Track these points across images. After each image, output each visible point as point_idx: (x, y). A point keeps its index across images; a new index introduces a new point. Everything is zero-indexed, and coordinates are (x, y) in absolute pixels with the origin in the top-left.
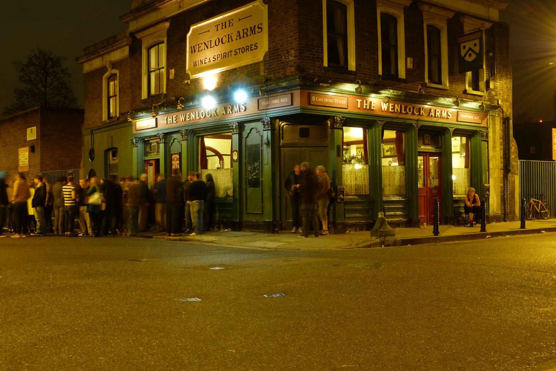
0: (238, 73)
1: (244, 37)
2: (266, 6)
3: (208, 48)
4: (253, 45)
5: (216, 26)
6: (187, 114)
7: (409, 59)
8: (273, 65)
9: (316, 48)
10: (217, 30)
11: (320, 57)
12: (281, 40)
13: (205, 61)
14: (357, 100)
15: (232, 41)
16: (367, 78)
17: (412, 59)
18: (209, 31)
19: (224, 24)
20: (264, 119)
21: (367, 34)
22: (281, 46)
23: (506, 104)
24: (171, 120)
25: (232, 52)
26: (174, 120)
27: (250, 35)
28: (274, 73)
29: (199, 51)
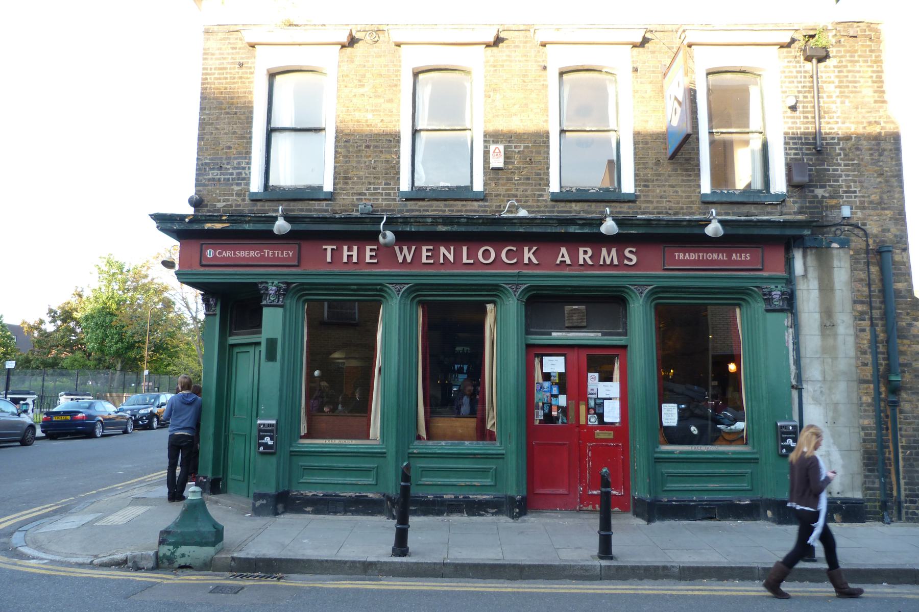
6: (424, 248)
24: (355, 253)
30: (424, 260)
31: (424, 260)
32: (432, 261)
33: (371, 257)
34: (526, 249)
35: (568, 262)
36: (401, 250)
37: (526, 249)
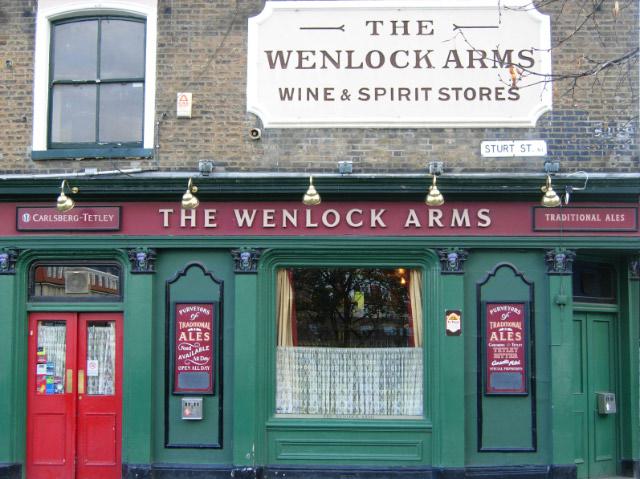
0: (450, 141)
1: (471, 66)
2: (546, 19)
3: (337, 65)
4: (503, 88)
5: (371, 25)
6: (266, 212)
8: (566, 141)
10: (375, 33)
13: (326, 94)
15: (430, 66)
18: (341, 28)
19: (400, 24)
20: (557, 249)
22: (590, 107)
25: (429, 92)
27: (495, 67)
28: (572, 159)
29: (300, 66)
30: (266, 224)
31: (266, 224)
32: (273, 225)
33: (211, 221)
34: (373, 211)
35: (418, 225)
36: (241, 214)
37: (373, 211)
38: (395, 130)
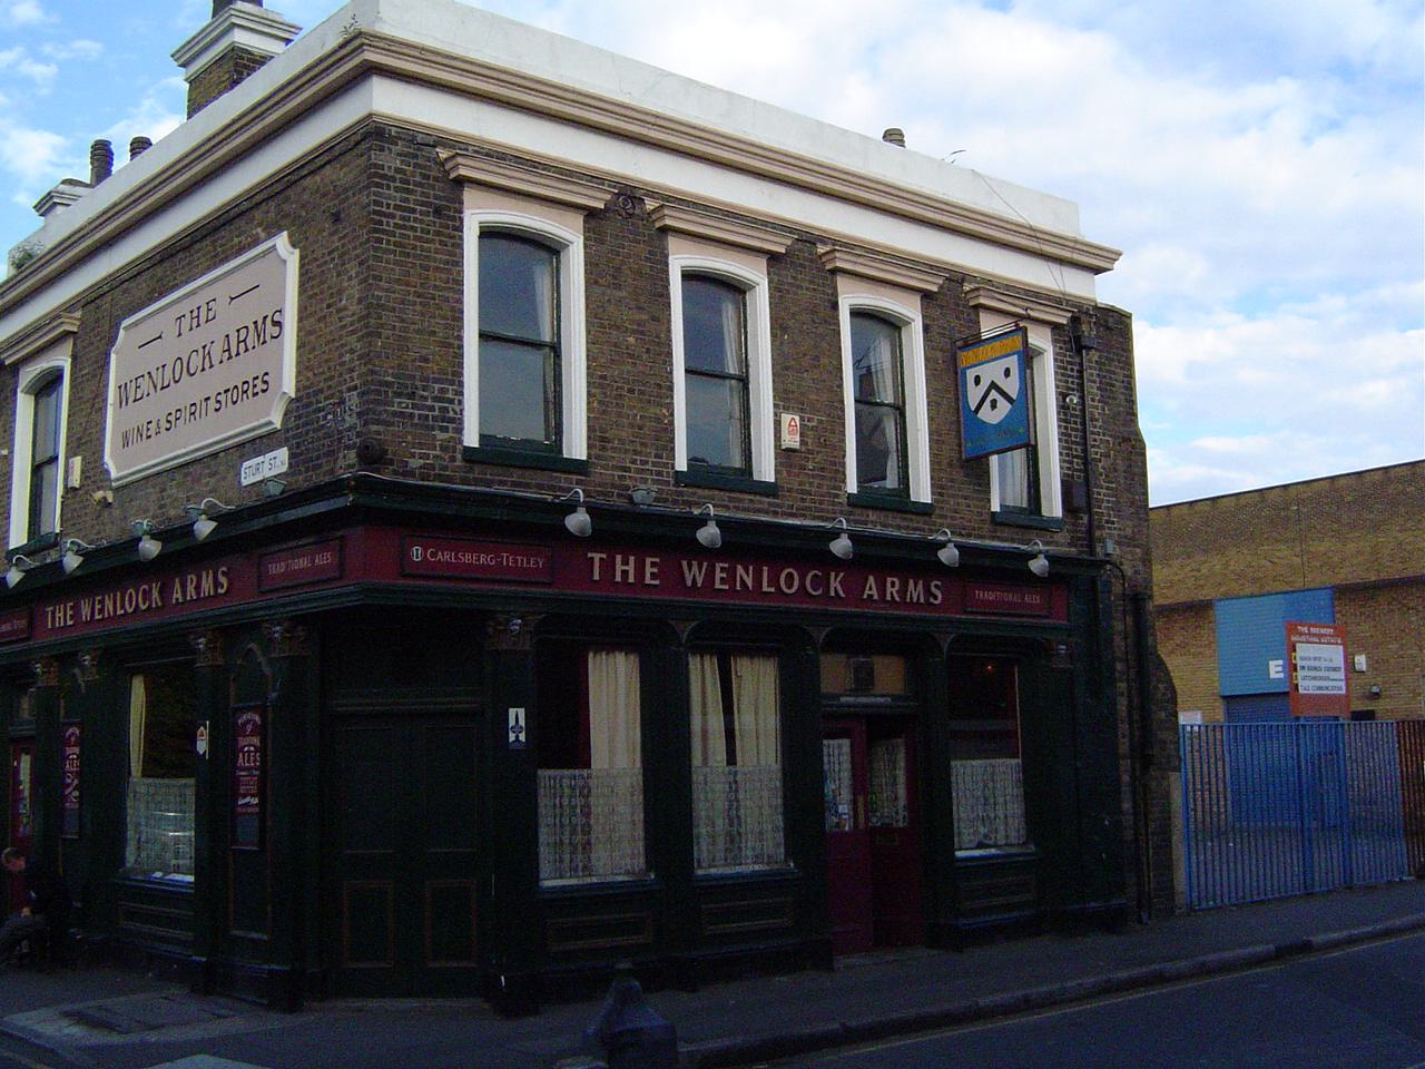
1: (238, 354)
2: (297, 251)
4: (257, 378)
7: (786, 418)
9: (437, 386)
11: (451, 414)
12: (326, 361)
13: (148, 429)
14: (590, 555)
16: (628, 482)
17: (797, 418)
21: (631, 340)
23: (1133, 554)
26: (68, 617)
28: (307, 470)
38: (187, 464)
